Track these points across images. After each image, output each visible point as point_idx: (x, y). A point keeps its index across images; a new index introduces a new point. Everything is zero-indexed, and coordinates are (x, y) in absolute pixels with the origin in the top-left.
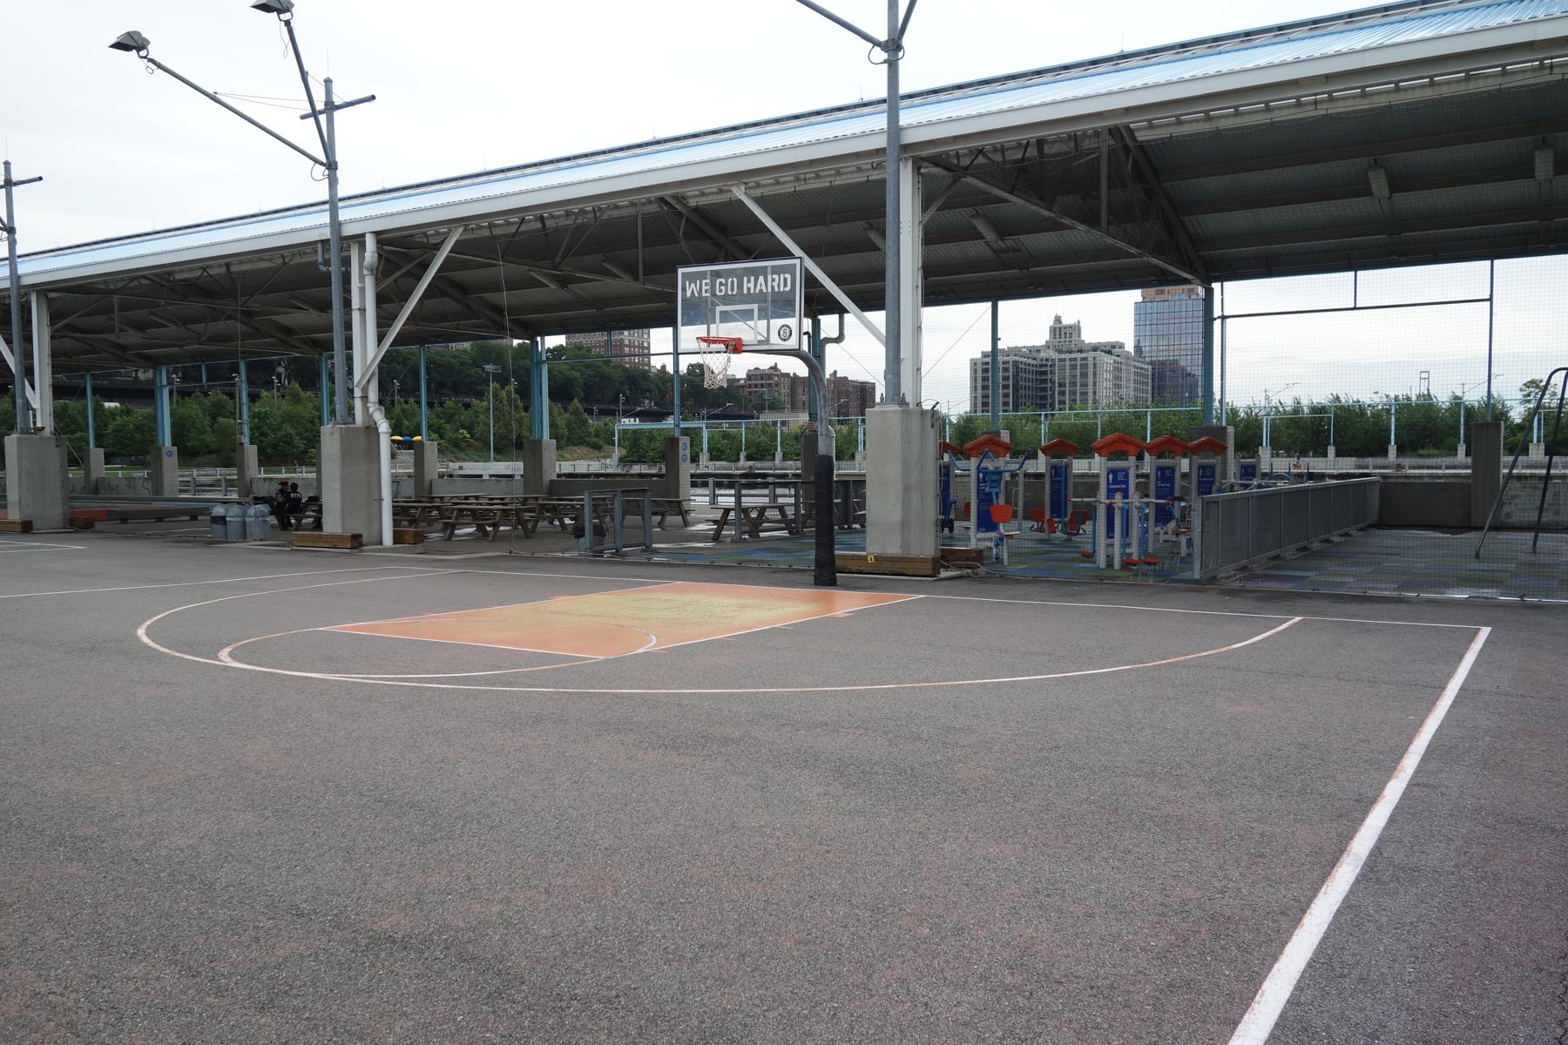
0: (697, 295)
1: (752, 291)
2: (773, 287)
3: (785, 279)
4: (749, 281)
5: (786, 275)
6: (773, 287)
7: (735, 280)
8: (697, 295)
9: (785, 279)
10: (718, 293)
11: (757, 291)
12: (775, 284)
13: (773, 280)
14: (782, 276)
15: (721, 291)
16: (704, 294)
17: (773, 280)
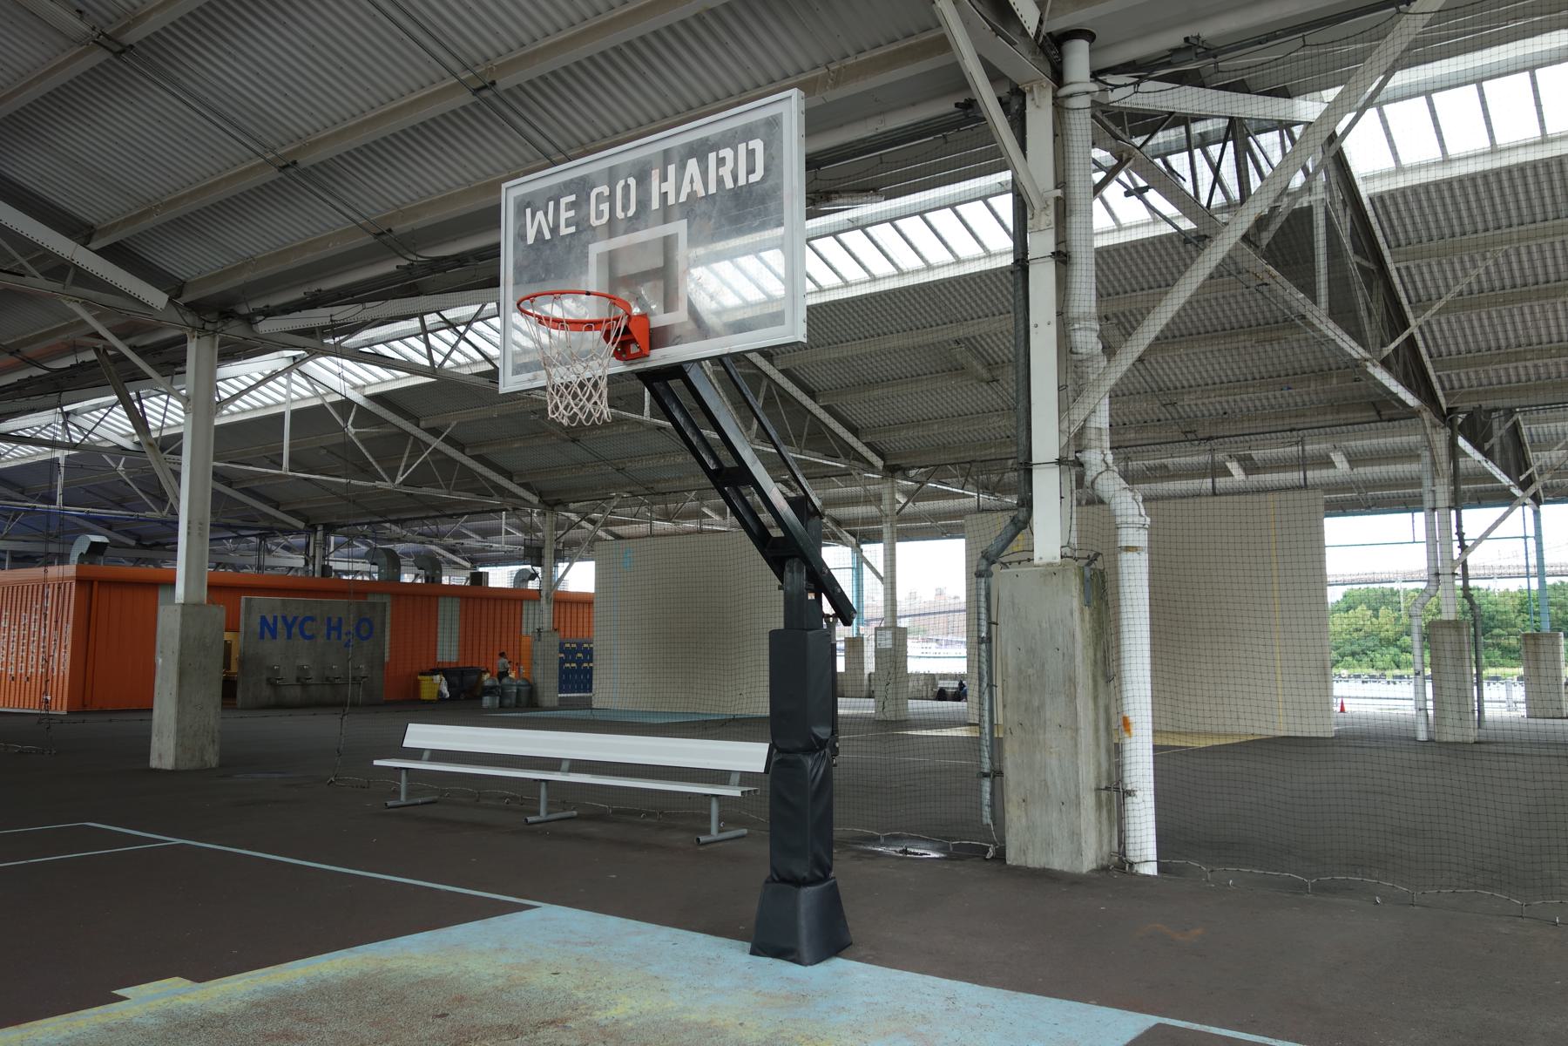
0: (548, 236)
1: (671, 200)
2: (720, 181)
3: (751, 154)
4: (664, 178)
5: (752, 144)
6: (720, 181)
7: (632, 182)
8: (548, 236)
9: (751, 154)
10: (594, 222)
11: (683, 198)
12: (726, 172)
13: (721, 162)
14: (742, 148)
15: (599, 215)
16: (564, 231)
17: (721, 162)
